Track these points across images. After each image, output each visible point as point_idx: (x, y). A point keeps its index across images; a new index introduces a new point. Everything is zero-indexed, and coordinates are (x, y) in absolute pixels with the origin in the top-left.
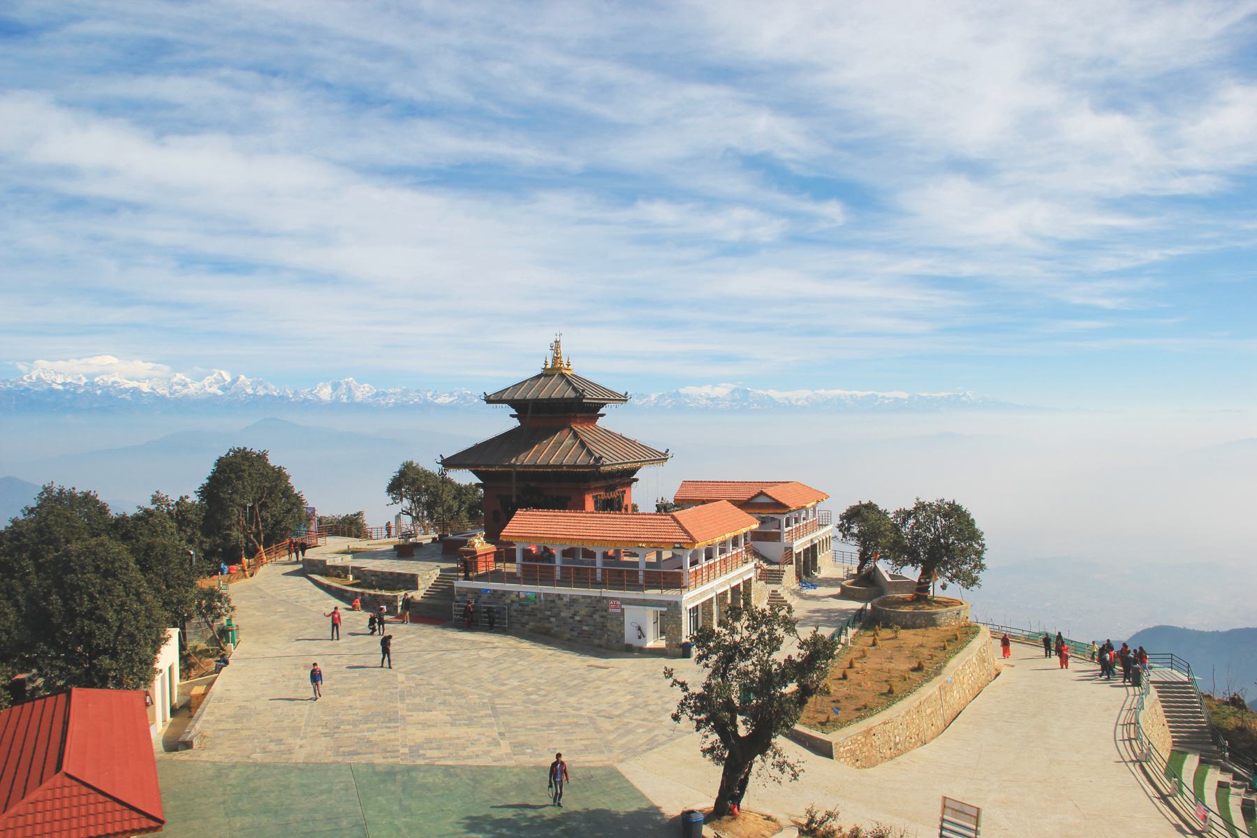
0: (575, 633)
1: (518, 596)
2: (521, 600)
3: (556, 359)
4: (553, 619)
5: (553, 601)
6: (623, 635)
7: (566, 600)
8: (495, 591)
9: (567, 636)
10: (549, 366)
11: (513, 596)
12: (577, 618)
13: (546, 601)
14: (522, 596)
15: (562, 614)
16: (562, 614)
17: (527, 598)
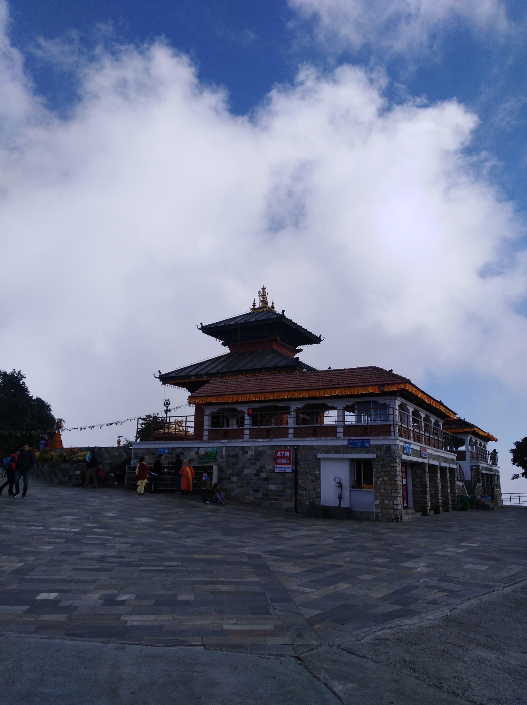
0: (260, 495)
1: (197, 453)
2: (200, 457)
3: (264, 301)
4: (234, 479)
5: (236, 456)
6: (319, 496)
7: (251, 453)
8: (173, 449)
9: (250, 498)
10: (257, 307)
11: (192, 454)
12: (263, 475)
13: (228, 456)
14: (202, 452)
15: (246, 471)
16: (246, 471)
17: (207, 455)
